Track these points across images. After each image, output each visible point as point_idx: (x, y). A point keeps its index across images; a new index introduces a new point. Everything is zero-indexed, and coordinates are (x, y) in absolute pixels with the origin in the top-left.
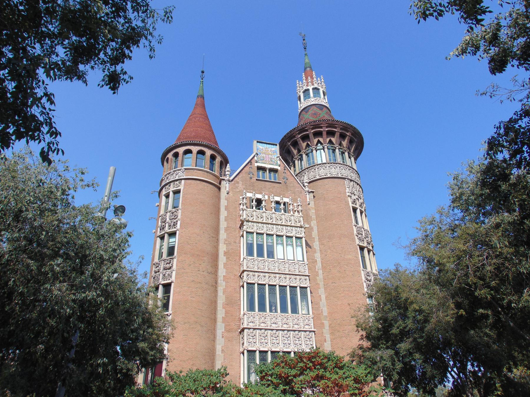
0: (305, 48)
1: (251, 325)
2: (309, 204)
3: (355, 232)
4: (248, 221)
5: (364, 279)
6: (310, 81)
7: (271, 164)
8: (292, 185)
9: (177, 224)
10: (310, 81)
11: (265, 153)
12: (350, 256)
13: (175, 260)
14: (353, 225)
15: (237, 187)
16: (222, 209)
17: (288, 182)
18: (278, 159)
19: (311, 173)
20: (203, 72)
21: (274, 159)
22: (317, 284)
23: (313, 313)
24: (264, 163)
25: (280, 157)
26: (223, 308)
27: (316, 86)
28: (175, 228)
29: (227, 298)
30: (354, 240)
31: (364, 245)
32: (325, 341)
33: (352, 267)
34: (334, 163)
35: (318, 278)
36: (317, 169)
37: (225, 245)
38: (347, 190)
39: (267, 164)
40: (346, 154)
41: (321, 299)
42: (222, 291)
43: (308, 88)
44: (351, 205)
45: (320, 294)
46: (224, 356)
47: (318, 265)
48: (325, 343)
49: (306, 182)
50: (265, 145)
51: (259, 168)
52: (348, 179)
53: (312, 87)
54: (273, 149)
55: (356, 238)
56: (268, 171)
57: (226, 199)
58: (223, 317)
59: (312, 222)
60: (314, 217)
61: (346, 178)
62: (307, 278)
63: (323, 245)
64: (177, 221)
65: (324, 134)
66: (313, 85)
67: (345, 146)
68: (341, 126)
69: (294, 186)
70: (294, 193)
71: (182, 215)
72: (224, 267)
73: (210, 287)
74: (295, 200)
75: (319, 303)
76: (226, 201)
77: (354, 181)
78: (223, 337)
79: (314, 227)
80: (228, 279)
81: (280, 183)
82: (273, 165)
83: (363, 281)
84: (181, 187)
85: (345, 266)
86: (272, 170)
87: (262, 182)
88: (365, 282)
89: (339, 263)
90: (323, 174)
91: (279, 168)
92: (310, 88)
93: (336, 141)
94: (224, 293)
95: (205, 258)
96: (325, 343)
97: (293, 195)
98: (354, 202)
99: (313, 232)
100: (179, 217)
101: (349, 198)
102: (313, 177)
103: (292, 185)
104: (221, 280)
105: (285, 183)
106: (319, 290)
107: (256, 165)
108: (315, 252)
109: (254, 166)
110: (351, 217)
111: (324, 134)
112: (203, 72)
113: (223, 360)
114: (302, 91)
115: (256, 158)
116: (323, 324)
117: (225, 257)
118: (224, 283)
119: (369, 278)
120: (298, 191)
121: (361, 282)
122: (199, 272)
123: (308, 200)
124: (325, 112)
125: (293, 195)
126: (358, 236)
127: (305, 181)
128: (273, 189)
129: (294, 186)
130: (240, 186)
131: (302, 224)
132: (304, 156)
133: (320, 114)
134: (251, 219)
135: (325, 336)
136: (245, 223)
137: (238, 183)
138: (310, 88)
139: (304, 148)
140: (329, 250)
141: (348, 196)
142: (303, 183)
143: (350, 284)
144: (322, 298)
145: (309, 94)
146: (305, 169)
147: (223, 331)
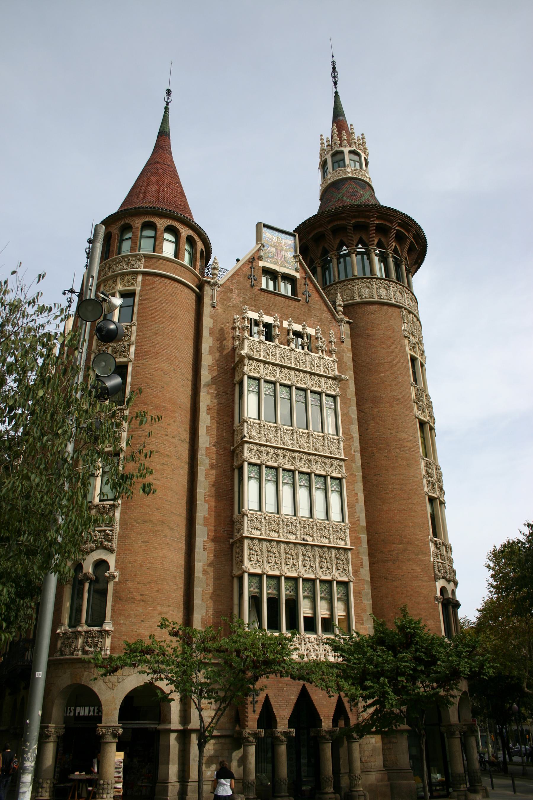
0: (335, 83)
1: (256, 534)
2: (343, 342)
3: (414, 397)
4: (251, 358)
5: (424, 472)
7: (285, 267)
9: (129, 350)
10: (345, 137)
11: (275, 247)
15: (230, 299)
16: (205, 333)
17: (311, 302)
20: (169, 92)
21: (289, 258)
23: (350, 522)
24: (273, 263)
25: (301, 257)
26: (206, 501)
28: (125, 357)
30: (412, 411)
31: (425, 420)
32: (362, 565)
33: (407, 452)
34: (385, 280)
37: (209, 396)
39: (279, 265)
41: (357, 500)
42: (204, 473)
43: (342, 149)
44: (409, 352)
45: (356, 492)
46: (207, 579)
47: (355, 444)
48: (361, 569)
49: (340, 305)
50: (276, 233)
51: (267, 272)
52: (406, 309)
53: (349, 149)
56: (280, 278)
57: (212, 317)
58: (205, 517)
60: (350, 364)
61: (403, 307)
62: (342, 463)
63: (363, 412)
64: (129, 345)
65: (373, 229)
68: (400, 220)
71: (137, 335)
73: (183, 464)
75: (354, 505)
76: (212, 321)
77: (413, 314)
78: (205, 549)
81: (300, 300)
82: (288, 268)
84: (138, 288)
85: (398, 450)
86: (287, 278)
87: (271, 295)
90: (367, 296)
91: (298, 275)
95: (176, 415)
96: (361, 569)
99: (348, 390)
100: (133, 338)
104: (202, 455)
106: (356, 485)
107: (261, 264)
108: (350, 422)
109: (258, 266)
111: (373, 229)
112: (169, 92)
113: (205, 586)
114: (331, 152)
116: (359, 538)
117: (209, 417)
119: (430, 471)
122: (167, 437)
126: (417, 404)
127: (337, 303)
128: (287, 309)
130: (236, 298)
131: (337, 373)
134: (256, 356)
135: (362, 558)
136: (246, 361)
137: (231, 291)
138: (346, 150)
141: (405, 337)
142: (335, 308)
145: (343, 160)
146: (336, 284)
147: (206, 539)
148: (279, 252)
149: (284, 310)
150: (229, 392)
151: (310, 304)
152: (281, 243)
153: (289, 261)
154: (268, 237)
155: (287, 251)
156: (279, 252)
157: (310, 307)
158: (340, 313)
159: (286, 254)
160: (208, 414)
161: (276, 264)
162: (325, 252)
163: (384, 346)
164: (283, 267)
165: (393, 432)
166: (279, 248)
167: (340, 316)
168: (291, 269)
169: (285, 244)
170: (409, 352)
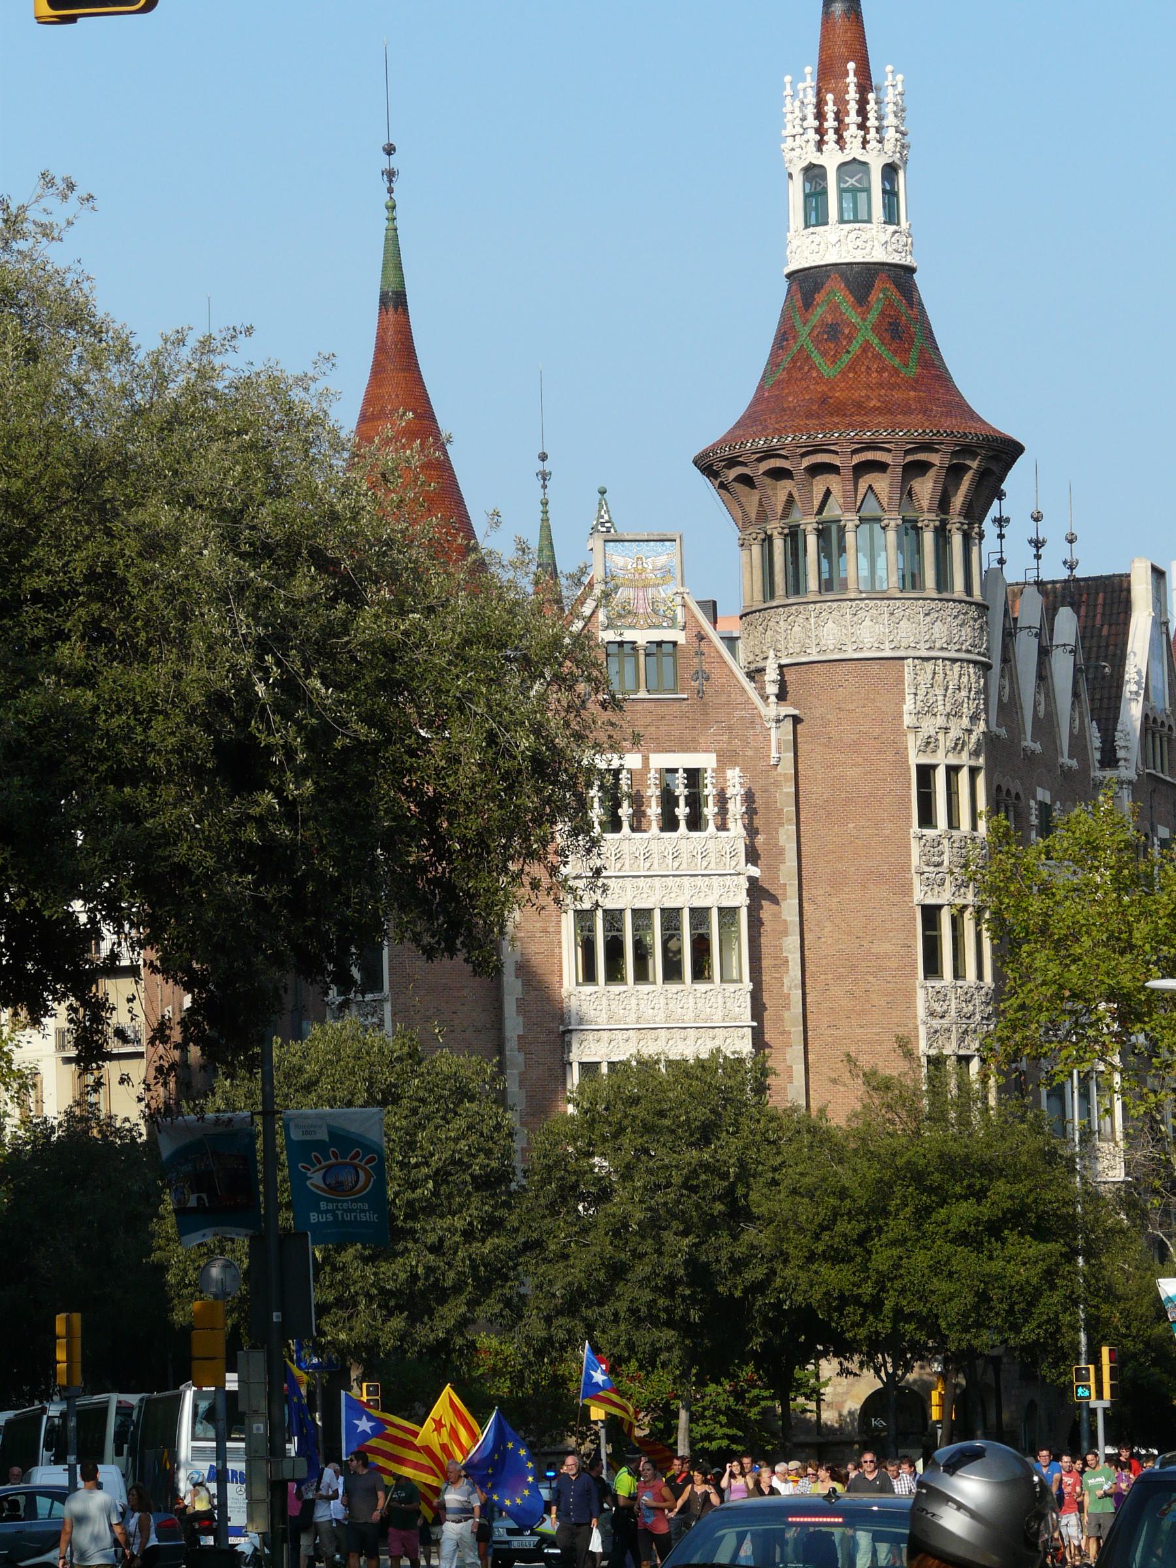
6: (830, 116)
8: (723, 699)
10: (830, 116)
11: (632, 584)
12: (887, 947)
13: (388, 1007)
14: (912, 835)
18: (679, 600)
19: (796, 629)
20: (390, 150)
22: (783, 1033)
27: (854, 150)
29: (530, 1098)
30: (907, 889)
35: (786, 1014)
36: (812, 620)
38: (908, 705)
40: (928, 538)
41: (791, 1077)
45: (789, 1063)
47: (791, 973)
54: (662, 560)
55: (916, 880)
59: (781, 831)
66: (840, 141)
67: (925, 504)
69: (728, 703)
70: (730, 728)
72: (518, 1012)
74: (726, 759)
75: (785, 1089)
79: (788, 846)
80: (530, 1044)
82: (660, 627)
83: (919, 1022)
85: (871, 979)
88: (925, 1023)
89: (853, 967)
91: (680, 637)
92: (831, 159)
93: (890, 498)
94: (522, 1084)
95: (464, 993)
97: (725, 738)
98: (929, 744)
99: (782, 866)
101: (911, 737)
102: (798, 650)
103: (723, 699)
104: (512, 1050)
105: (700, 693)
106: (789, 1050)
108: (785, 933)
110: (909, 808)
115: (601, 616)
117: (519, 982)
118: (520, 1058)
120: (742, 718)
121: (911, 1025)
123: (774, 754)
124: (873, 316)
125: (725, 738)
129: (728, 703)
132: (778, 544)
133: (850, 339)
138: (831, 159)
139: (779, 509)
140: (828, 924)
143: (878, 1034)
144: (794, 1074)
148: (641, 594)
149: (652, 729)
150: (552, 929)
151: (706, 699)
152: (644, 570)
153: (662, 608)
154: (616, 567)
155: (658, 585)
156: (641, 594)
157: (705, 704)
158: (773, 699)
159: (655, 592)
160: (517, 977)
161: (634, 627)
162: (763, 516)
163: (860, 760)
164: (650, 627)
165: (865, 943)
166: (640, 584)
167: (773, 709)
168: (664, 628)
169: (654, 569)
170: (915, 759)
